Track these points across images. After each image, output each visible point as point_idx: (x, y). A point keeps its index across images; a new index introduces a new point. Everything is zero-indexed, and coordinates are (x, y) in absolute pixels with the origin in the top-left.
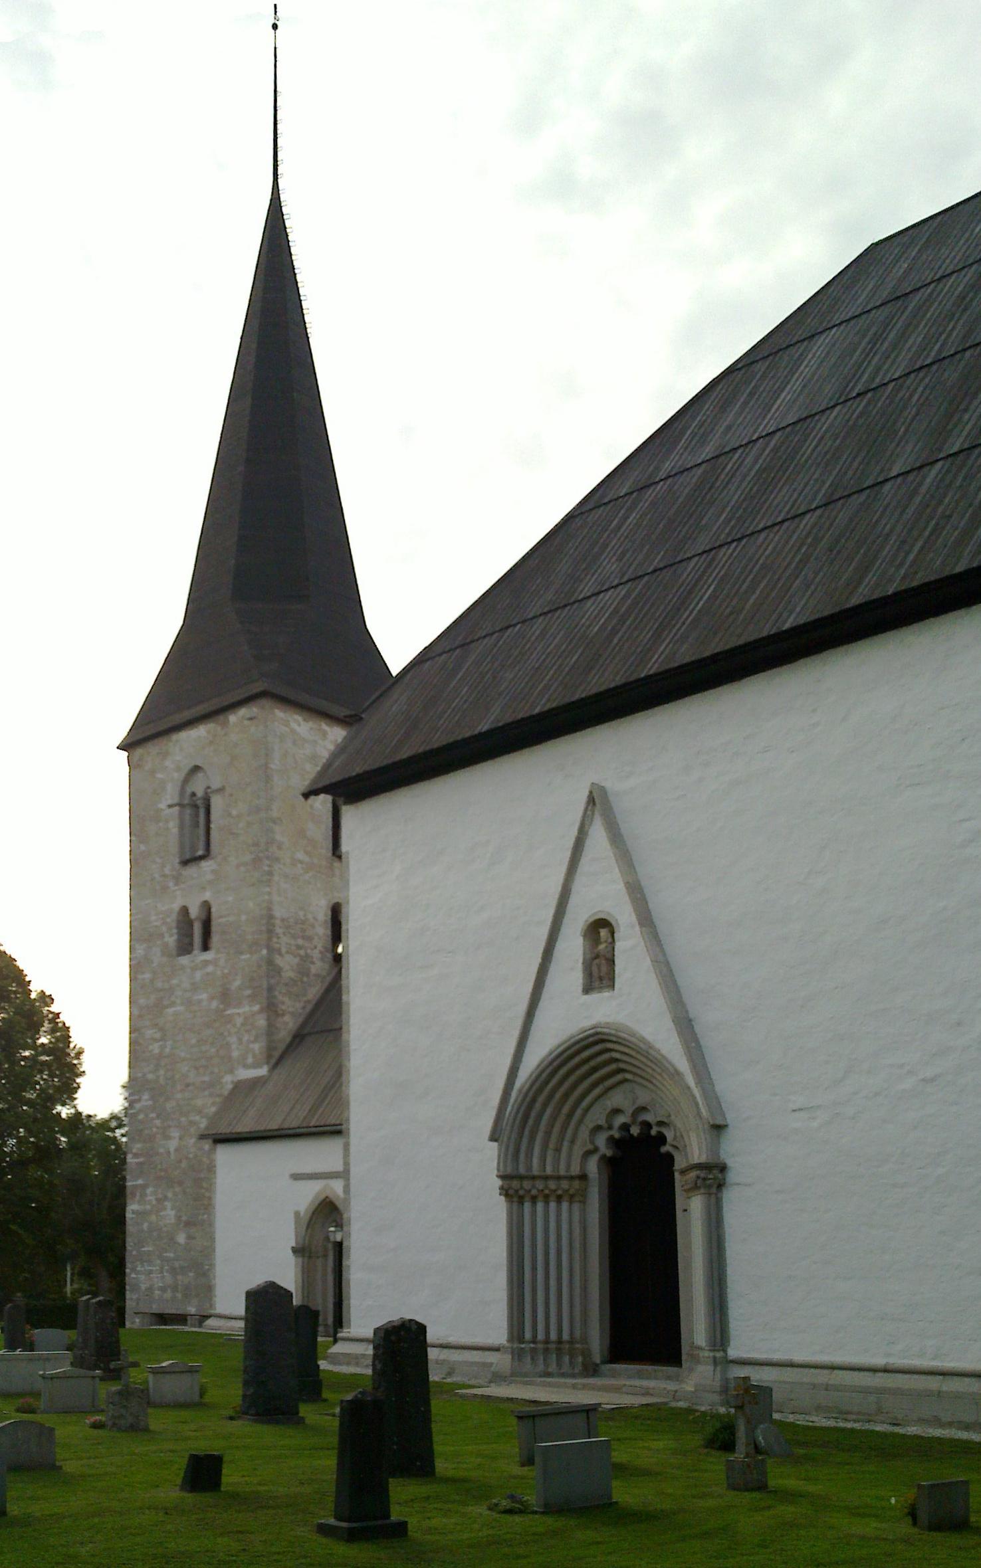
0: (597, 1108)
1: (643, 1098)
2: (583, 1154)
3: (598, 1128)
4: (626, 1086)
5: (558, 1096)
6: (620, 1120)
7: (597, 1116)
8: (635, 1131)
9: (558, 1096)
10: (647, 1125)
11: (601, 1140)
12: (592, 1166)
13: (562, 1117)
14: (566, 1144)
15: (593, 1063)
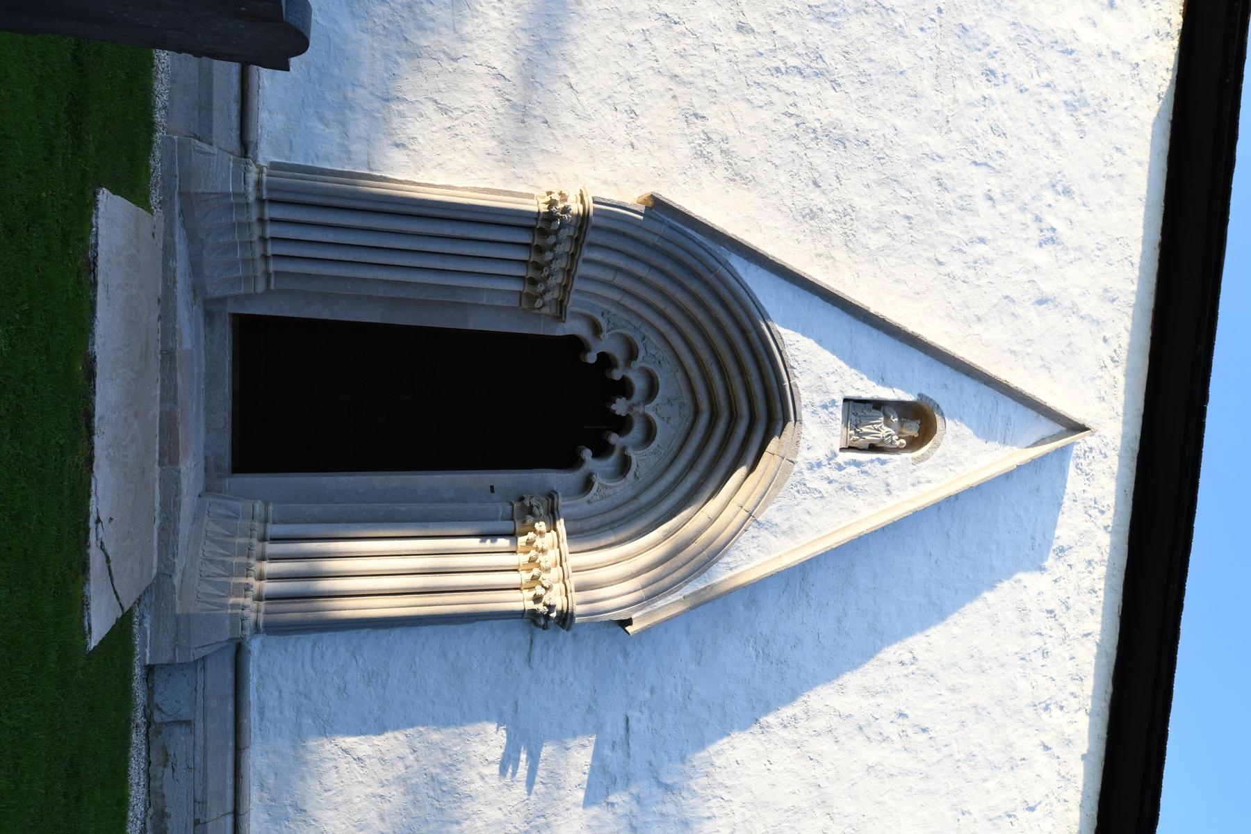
0: (664, 354)
1: (666, 433)
2: (592, 310)
3: (632, 354)
4: (688, 411)
5: (701, 316)
6: (639, 384)
7: (652, 355)
8: (620, 407)
9: (701, 316)
10: (623, 425)
11: (607, 344)
12: (573, 327)
13: (661, 305)
14: (617, 296)
15: (737, 382)
